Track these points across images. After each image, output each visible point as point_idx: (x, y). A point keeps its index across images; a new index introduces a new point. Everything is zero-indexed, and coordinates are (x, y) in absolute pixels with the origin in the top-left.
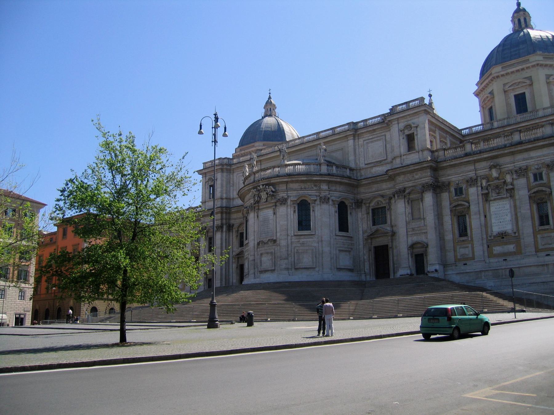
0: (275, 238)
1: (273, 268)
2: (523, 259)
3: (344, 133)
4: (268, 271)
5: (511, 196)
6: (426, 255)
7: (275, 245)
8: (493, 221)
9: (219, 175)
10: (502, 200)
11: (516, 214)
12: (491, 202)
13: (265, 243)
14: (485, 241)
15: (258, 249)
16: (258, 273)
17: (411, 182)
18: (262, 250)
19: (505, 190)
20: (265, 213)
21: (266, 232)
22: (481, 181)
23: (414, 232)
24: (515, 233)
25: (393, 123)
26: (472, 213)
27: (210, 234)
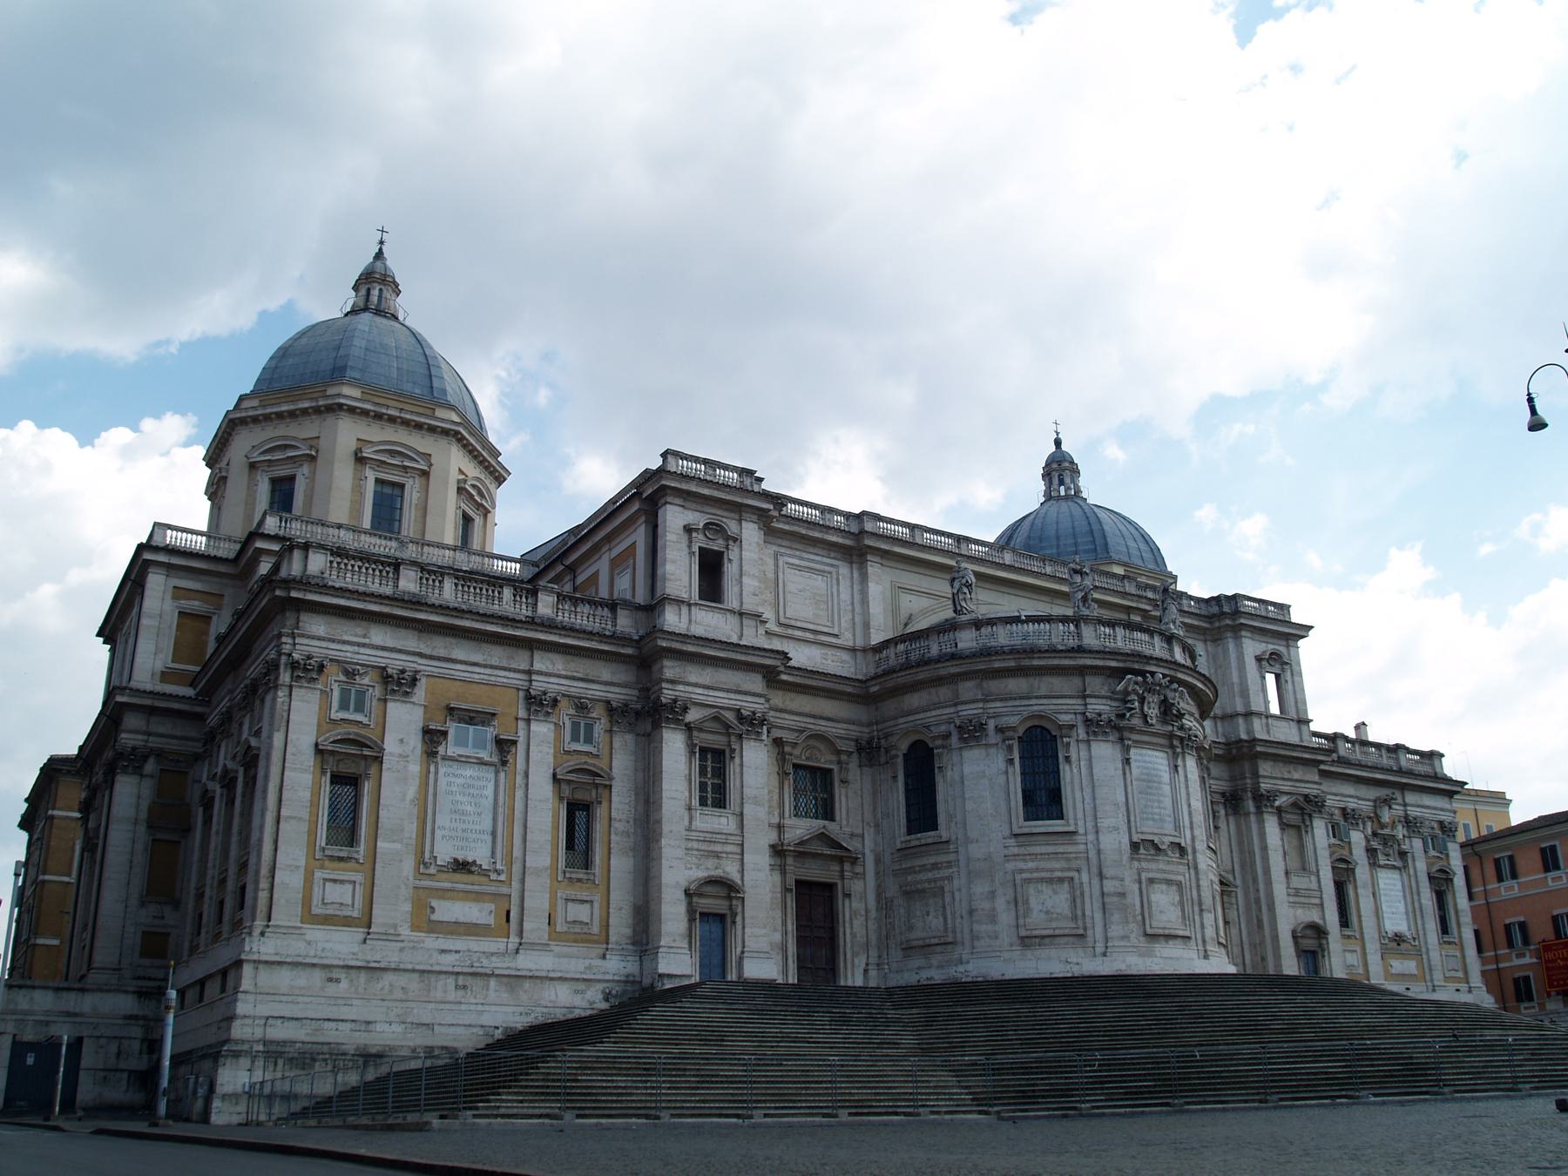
0: (1183, 845)
1: (1187, 933)
2: (1434, 990)
3: (1136, 599)
4: (1176, 937)
5: (1404, 867)
6: (1323, 956)
7: (1181, 864)
8: (1384, 908)
9: (750, 532)
10: (1392, 871)
11: (1413, 902)
12: (1378, 869)
13: (1160, 850)
14: (1378, 946)
15: (1136, 864)
16: (1142, 939)
17: (1289, 783)
18: (1156, 867)
19: (1396, 852)
20: (1147, 759)
21: (1156, 817)
22: (1364, 823)
23: (1297, 899)
24: (1414, 939)
25: (1243, 633)
26: (1359, 883)
27: (715, 740)
